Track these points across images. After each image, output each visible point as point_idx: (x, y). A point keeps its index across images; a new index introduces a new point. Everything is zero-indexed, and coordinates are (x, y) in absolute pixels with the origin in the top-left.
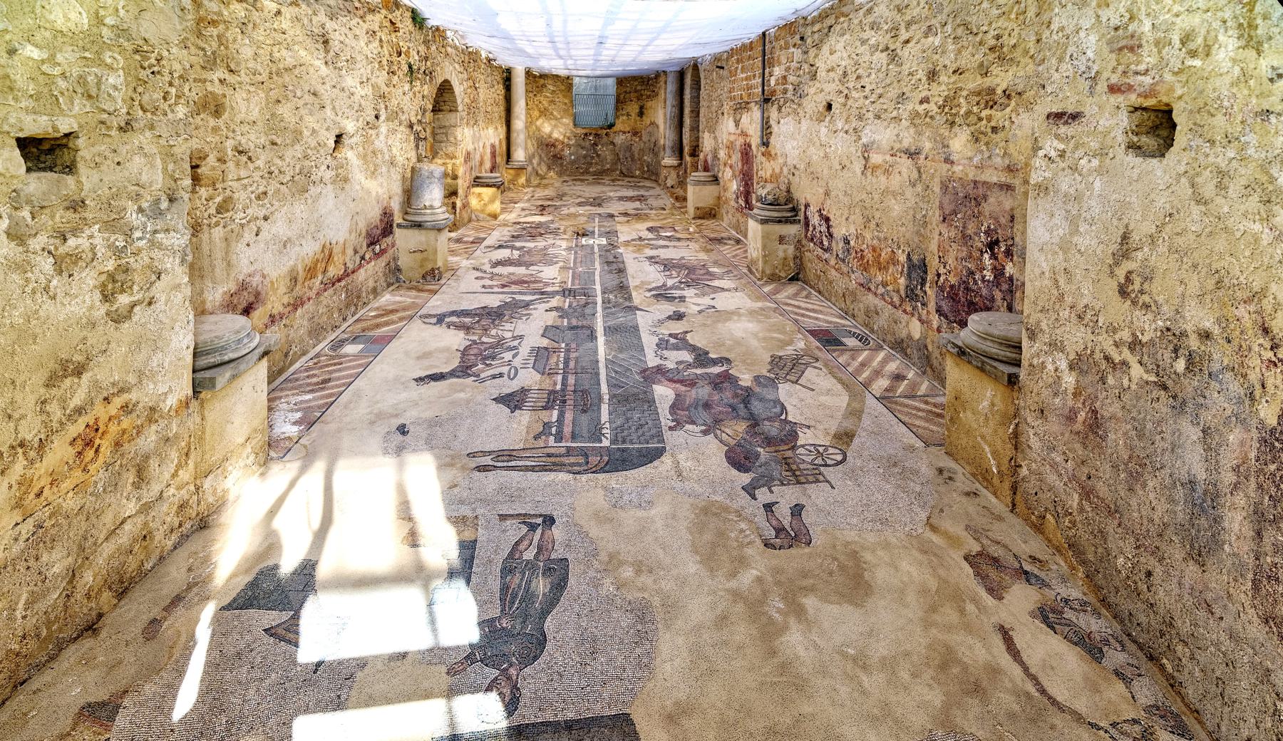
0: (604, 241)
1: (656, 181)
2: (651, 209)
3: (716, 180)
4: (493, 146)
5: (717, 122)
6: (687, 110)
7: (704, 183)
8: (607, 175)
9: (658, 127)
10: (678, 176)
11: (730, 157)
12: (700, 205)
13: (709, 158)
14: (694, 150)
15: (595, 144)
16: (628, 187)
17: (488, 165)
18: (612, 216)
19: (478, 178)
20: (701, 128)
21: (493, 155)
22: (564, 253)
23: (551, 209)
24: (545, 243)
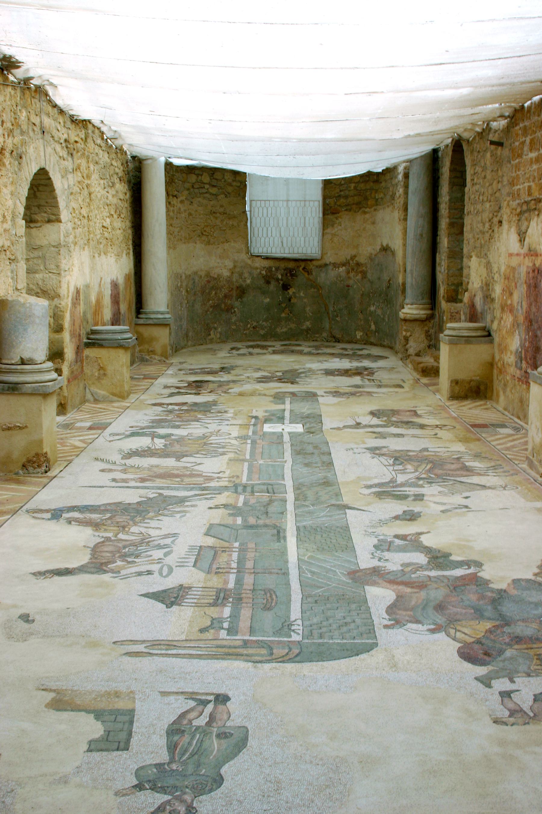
0: (299, 428)
1: (391, 348)
2: (380, 386)
3: (488, 335)
4: (115, 285)
5: (491, 237)
6: (444, 224)
7: (468, 340)
8: (306, 339)
9: (393, 253)
10: (428, 336)
11: (511, 294)
12: (461, 376)
13: (479, 301)
14: (456, 292)
15: (286, 287)
16: (341, 356)
17: (107, 314)
18: (315, 395)
19: (94, 332)
20: (465, 250)
21: (115, 300)
22: (234, 442)
23: (211, 386)
24: (204, 431)
